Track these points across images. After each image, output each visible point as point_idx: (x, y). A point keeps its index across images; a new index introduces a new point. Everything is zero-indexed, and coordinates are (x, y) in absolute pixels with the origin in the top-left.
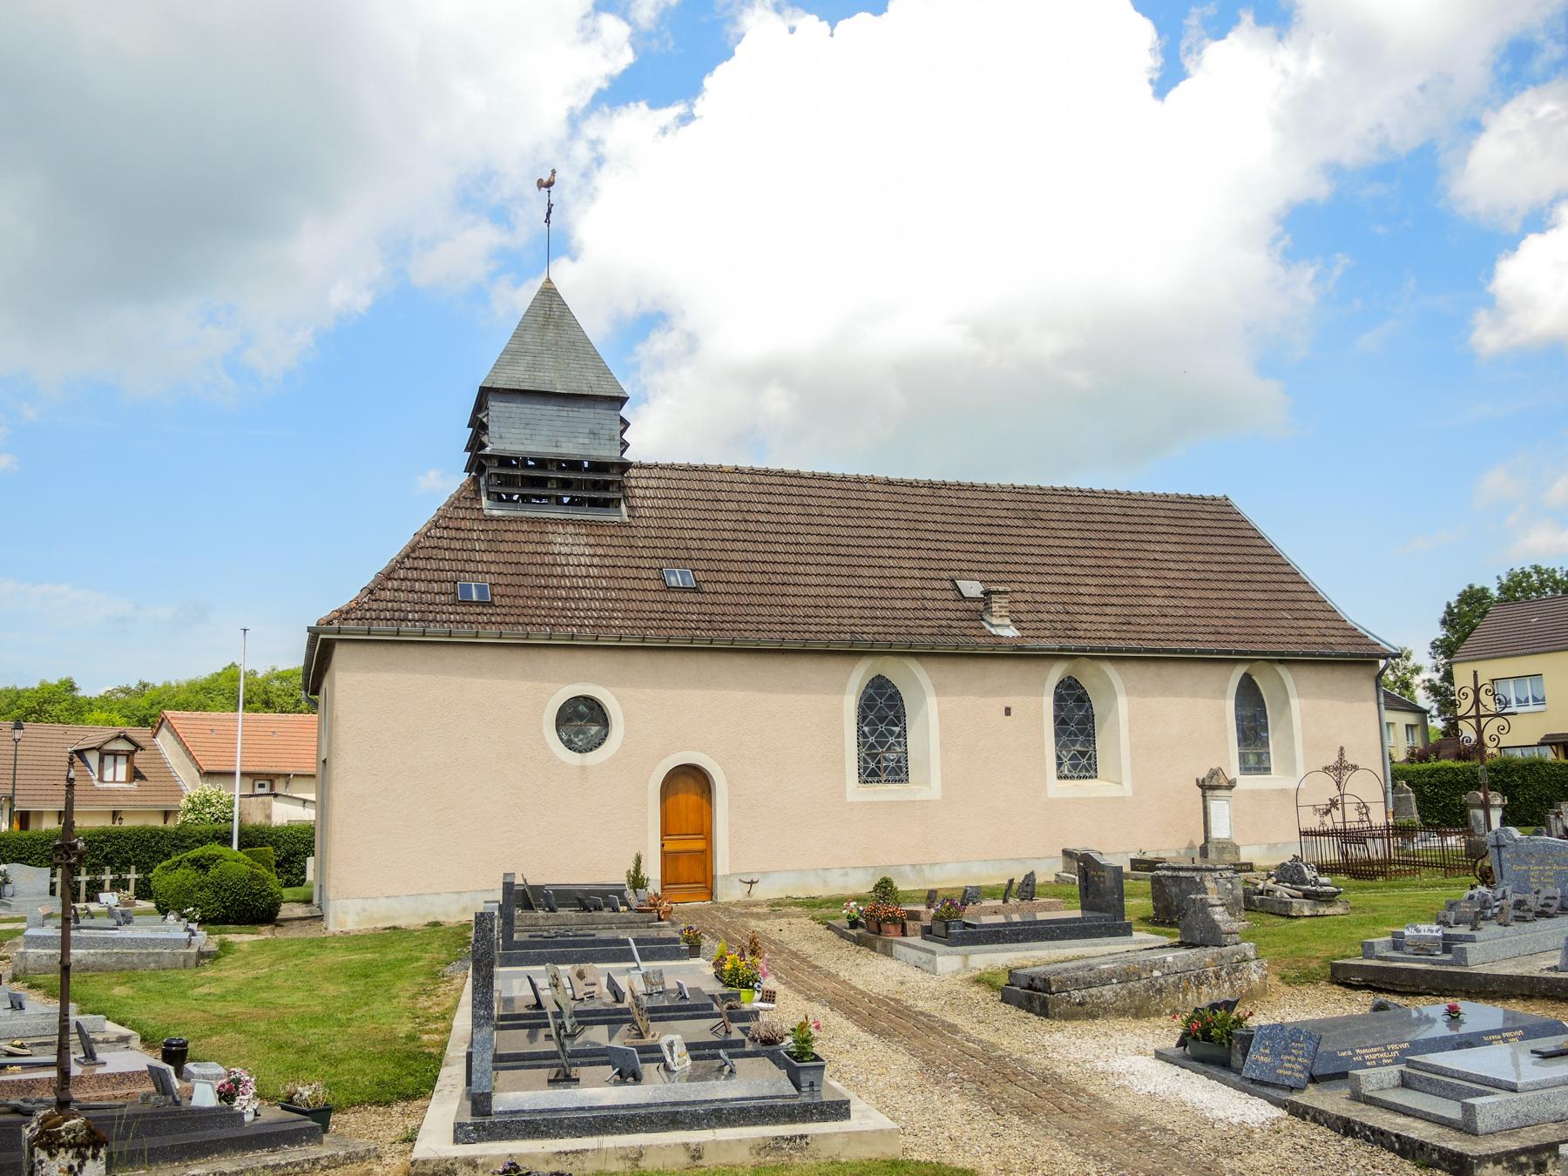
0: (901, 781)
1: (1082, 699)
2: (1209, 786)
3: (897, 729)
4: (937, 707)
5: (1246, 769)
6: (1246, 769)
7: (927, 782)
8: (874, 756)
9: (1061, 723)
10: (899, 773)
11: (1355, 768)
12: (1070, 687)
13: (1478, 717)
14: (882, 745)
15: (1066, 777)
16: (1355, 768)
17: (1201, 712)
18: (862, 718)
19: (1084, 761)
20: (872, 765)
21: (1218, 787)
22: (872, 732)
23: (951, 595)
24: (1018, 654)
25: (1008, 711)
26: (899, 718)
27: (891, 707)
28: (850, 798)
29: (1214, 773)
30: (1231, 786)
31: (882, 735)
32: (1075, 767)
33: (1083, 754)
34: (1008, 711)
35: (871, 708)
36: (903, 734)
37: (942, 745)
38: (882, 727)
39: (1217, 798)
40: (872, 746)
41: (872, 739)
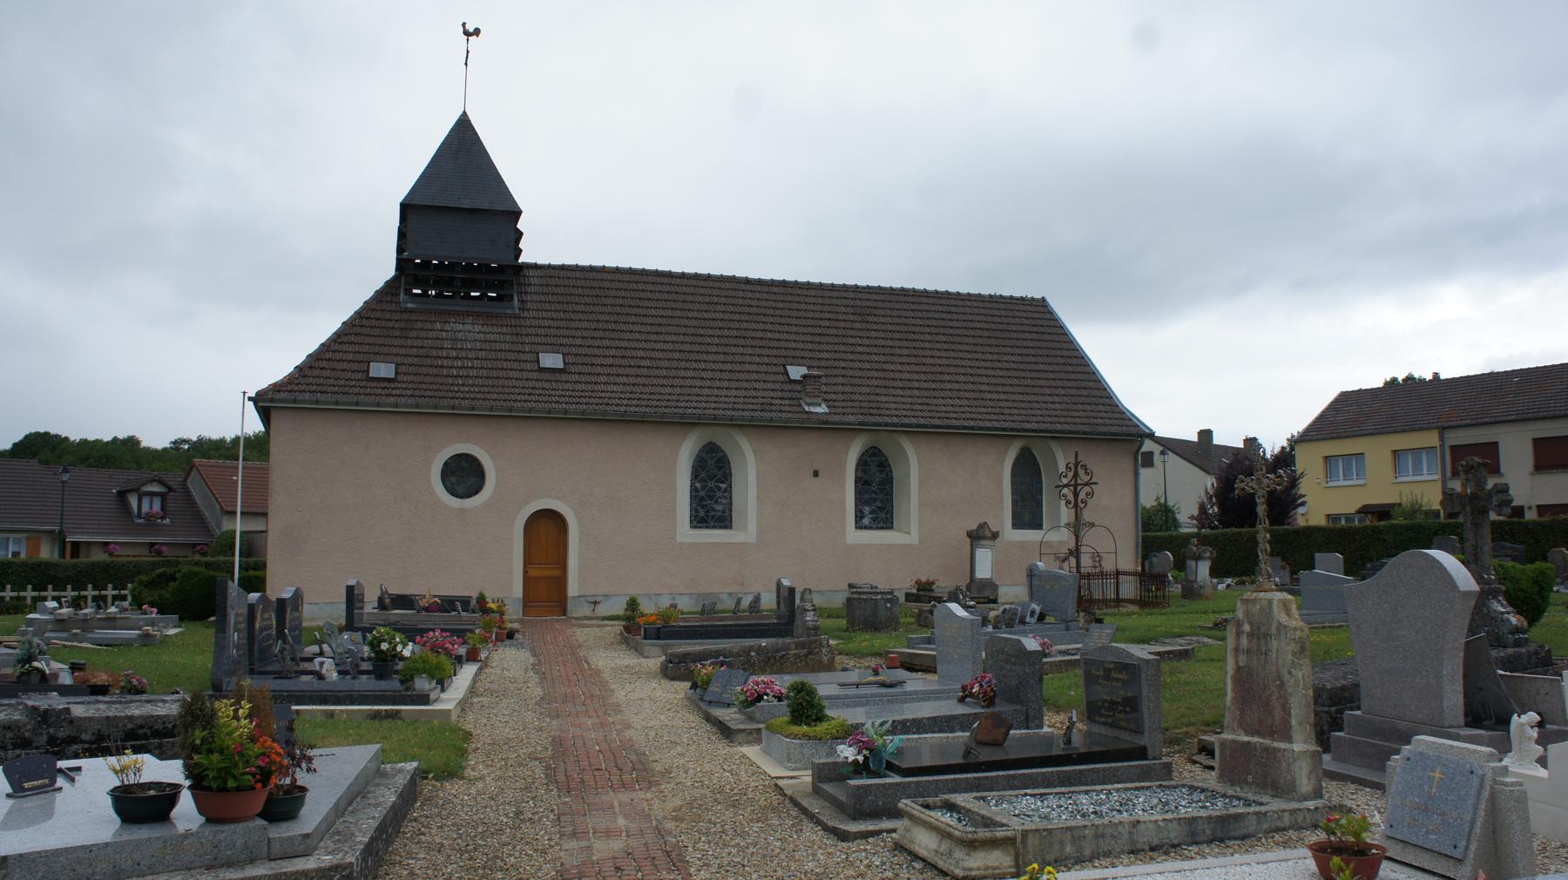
0: (726, 527)
1: (884, 466)
2: (978, 536)
3: (723, 486)
4: (753, 469)
5: (1018, 523)
6: (1018, 523)
7: (744, 528)
8: (704, 506)
9: (862, 484)
10: (724, 521)
11: (1092, 525)
12: (874, 455)
13: (1076, 486)
14: (711, 498)
15: (866, 528)
16: (1092, 525)
17: (987, 479)
18: (695, 476)
19: (883, 515)
20: (702, 513)
21: (984, 538)
22: (703, 488)
23: (781, 378)
24: (823, 427)
25: (816, 474)
26: (727, 476)
27: (719, 468)
28: (679, 539)
29: (983, 526)
30: (995, 536)
31: (711, 490)
32: (874, 519)
33: (880, 509)
34: (816, 474)
35: (703, 468)
36: (729, 490)
37: (758, 498)
38: (711, 484)
39: (983, 547)
40: (702, 499)
41: (702, 493)
